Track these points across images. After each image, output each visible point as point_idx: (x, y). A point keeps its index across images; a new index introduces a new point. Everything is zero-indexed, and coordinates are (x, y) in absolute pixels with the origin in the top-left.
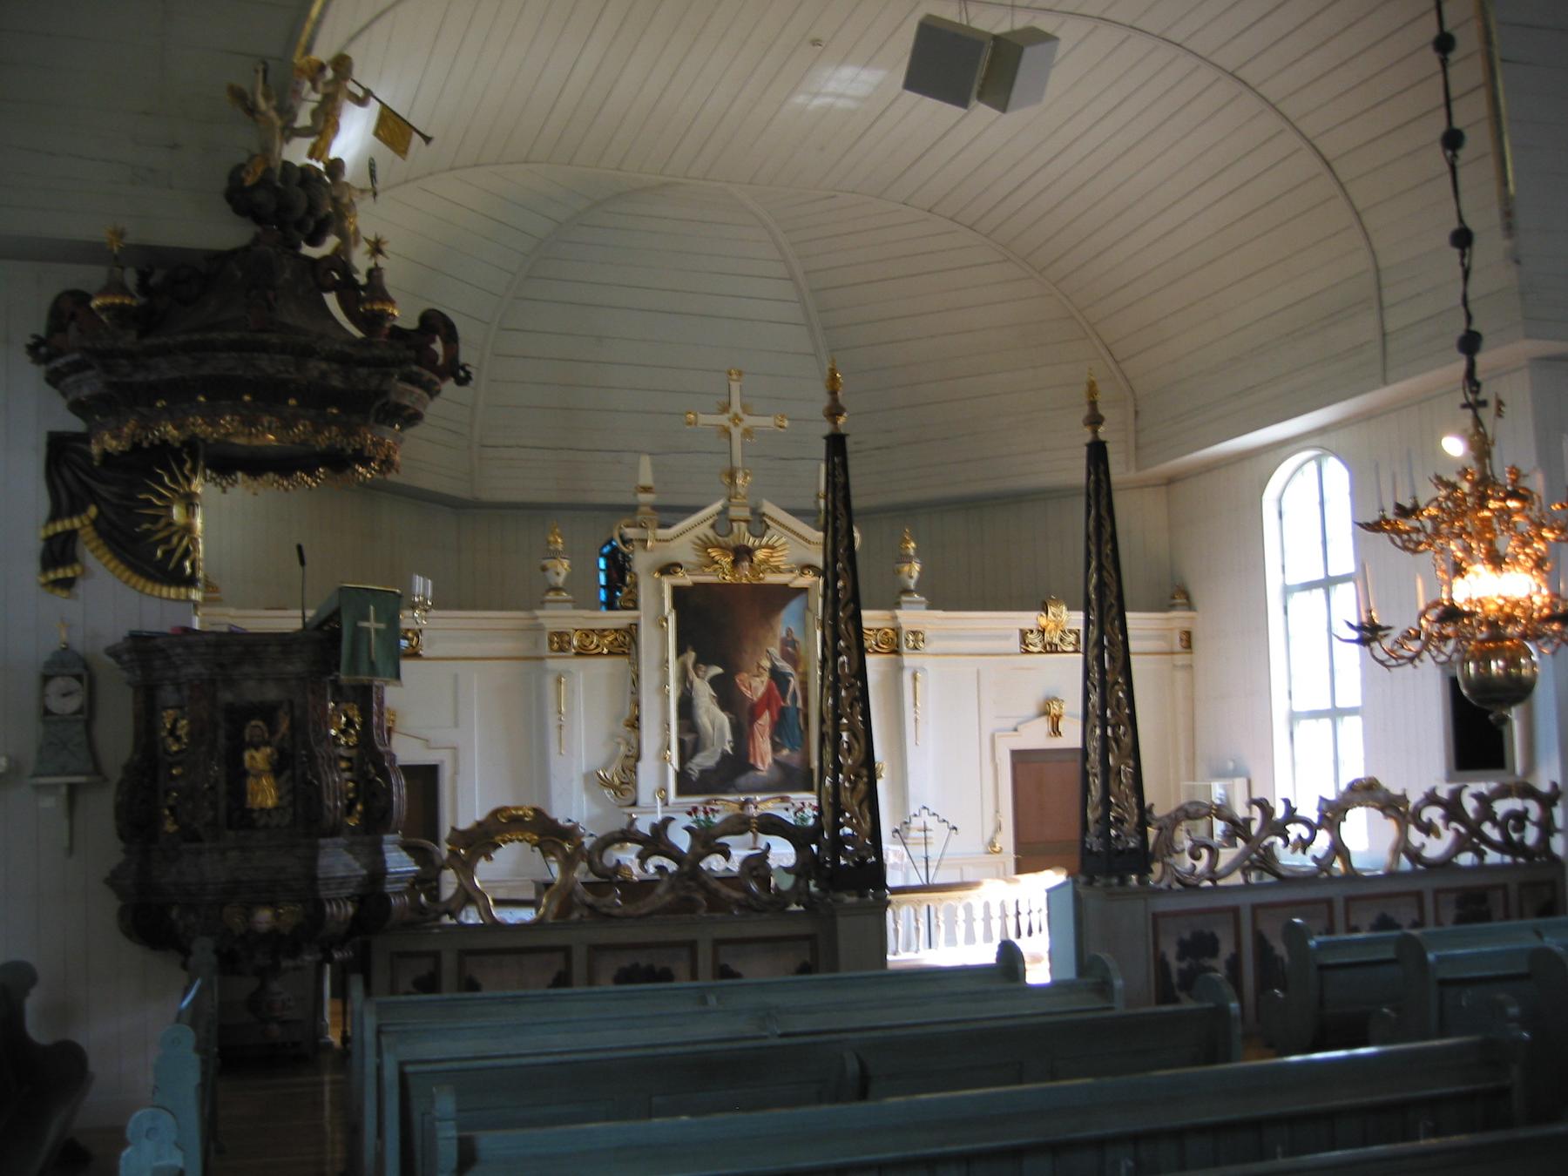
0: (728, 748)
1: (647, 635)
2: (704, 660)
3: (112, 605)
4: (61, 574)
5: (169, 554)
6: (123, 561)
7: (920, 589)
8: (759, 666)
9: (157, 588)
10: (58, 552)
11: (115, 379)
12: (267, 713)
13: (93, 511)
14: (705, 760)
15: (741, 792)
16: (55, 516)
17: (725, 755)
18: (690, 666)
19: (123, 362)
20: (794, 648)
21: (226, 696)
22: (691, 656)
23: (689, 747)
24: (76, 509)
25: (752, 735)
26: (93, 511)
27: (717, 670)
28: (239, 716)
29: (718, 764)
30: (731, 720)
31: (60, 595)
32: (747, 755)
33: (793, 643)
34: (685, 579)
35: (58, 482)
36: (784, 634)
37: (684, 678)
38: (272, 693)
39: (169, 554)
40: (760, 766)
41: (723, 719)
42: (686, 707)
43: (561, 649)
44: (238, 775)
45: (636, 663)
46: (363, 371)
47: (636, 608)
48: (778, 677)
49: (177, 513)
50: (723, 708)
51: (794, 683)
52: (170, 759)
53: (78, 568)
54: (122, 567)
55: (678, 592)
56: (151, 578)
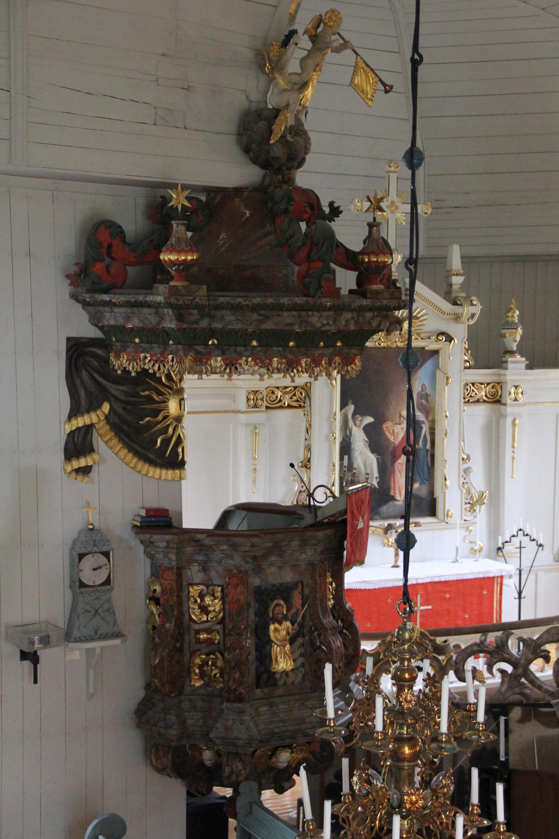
3: (118, 485)
4: (83, 462)
5: (166, 442)
6: (131, 449)
7: (521, 351)
9: (158, 471)
10: (78, 446)
11: (185, 326)
12: (284, 592)
13: (106, 407)
15: (384, 518)
16: (74, 413)
18: (350, 416)
19: (195, 312)
20: (427, 401)
21: (256, 581)
22: (351, 408)
24: (93, 407)
25: (393, 471)
26: (106, 407)
27: (369, 420)
28: (265, 596)
30: (377, 459)
31: (80, 482)
32: (389, 489)
35: (78, 382)
36: (420, 390)
37: (345, 426)
38: (288, 577)
39: (166, 442)
40: (398, 497)
41: (372, 459)
43: (256, 406)
44: (264, 644)
45: (308, 415)
46: (369, 315)
48: (413, 424)
49: (173, 407)
50: (373, 451)
51: (425, 429)
52: (196, 627)
53: (95, 456)
54: (130, 455)
56: (152, 463)
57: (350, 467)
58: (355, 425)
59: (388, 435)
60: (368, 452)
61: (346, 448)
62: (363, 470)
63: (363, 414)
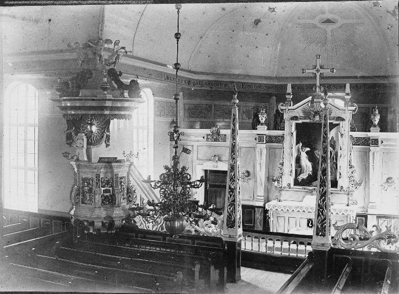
0: (311, 173)
1: (287, 138)
14: (304, 176)
17: (309, 175)
18: (300, 148)
23: (299, 172)
27: (308, 149)
33: (334, 142)
34: (300, 121)
41: (309, 164)
42: (298, 160)
50: (310, 161)
55: (296, 124)
57: (300, 166)
60: (308, 161)
61: (298, 160)
63: (306, 147)
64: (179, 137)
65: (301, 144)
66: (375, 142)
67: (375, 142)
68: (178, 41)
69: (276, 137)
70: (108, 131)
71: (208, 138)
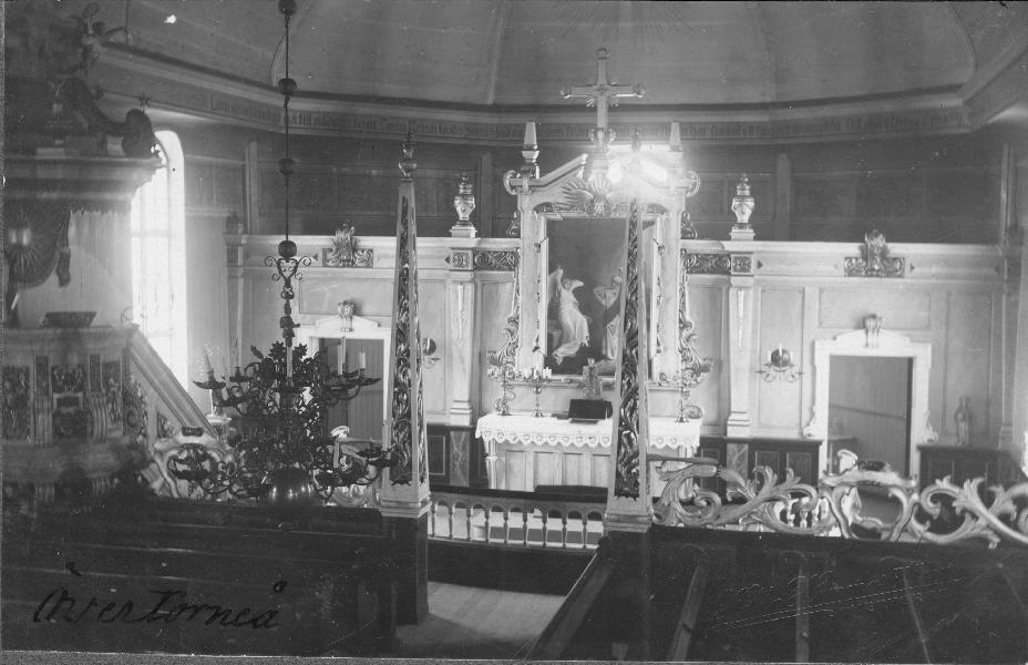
0: (586, 342)
2: (570, 275)
8: (613, 281)
17: (582, 349)
23: (555, 344)
29: (577, 353)
30: (588, 321)
32: (600, 349)
34: (558, 217)
37: (554, 288)
40: (610, 355)
47: (518, 236)
55: (551, 225)
58: (564, 287)
59: (599, 298)
62: (572, 329)
63: (573, 278)
64: (296, 268)
65: (562, 271)
66: (744, 263)
67: (744, 263)
68: (287, 21)
69: (501, 255)
70: (66, 243)
71: (325, 260)
